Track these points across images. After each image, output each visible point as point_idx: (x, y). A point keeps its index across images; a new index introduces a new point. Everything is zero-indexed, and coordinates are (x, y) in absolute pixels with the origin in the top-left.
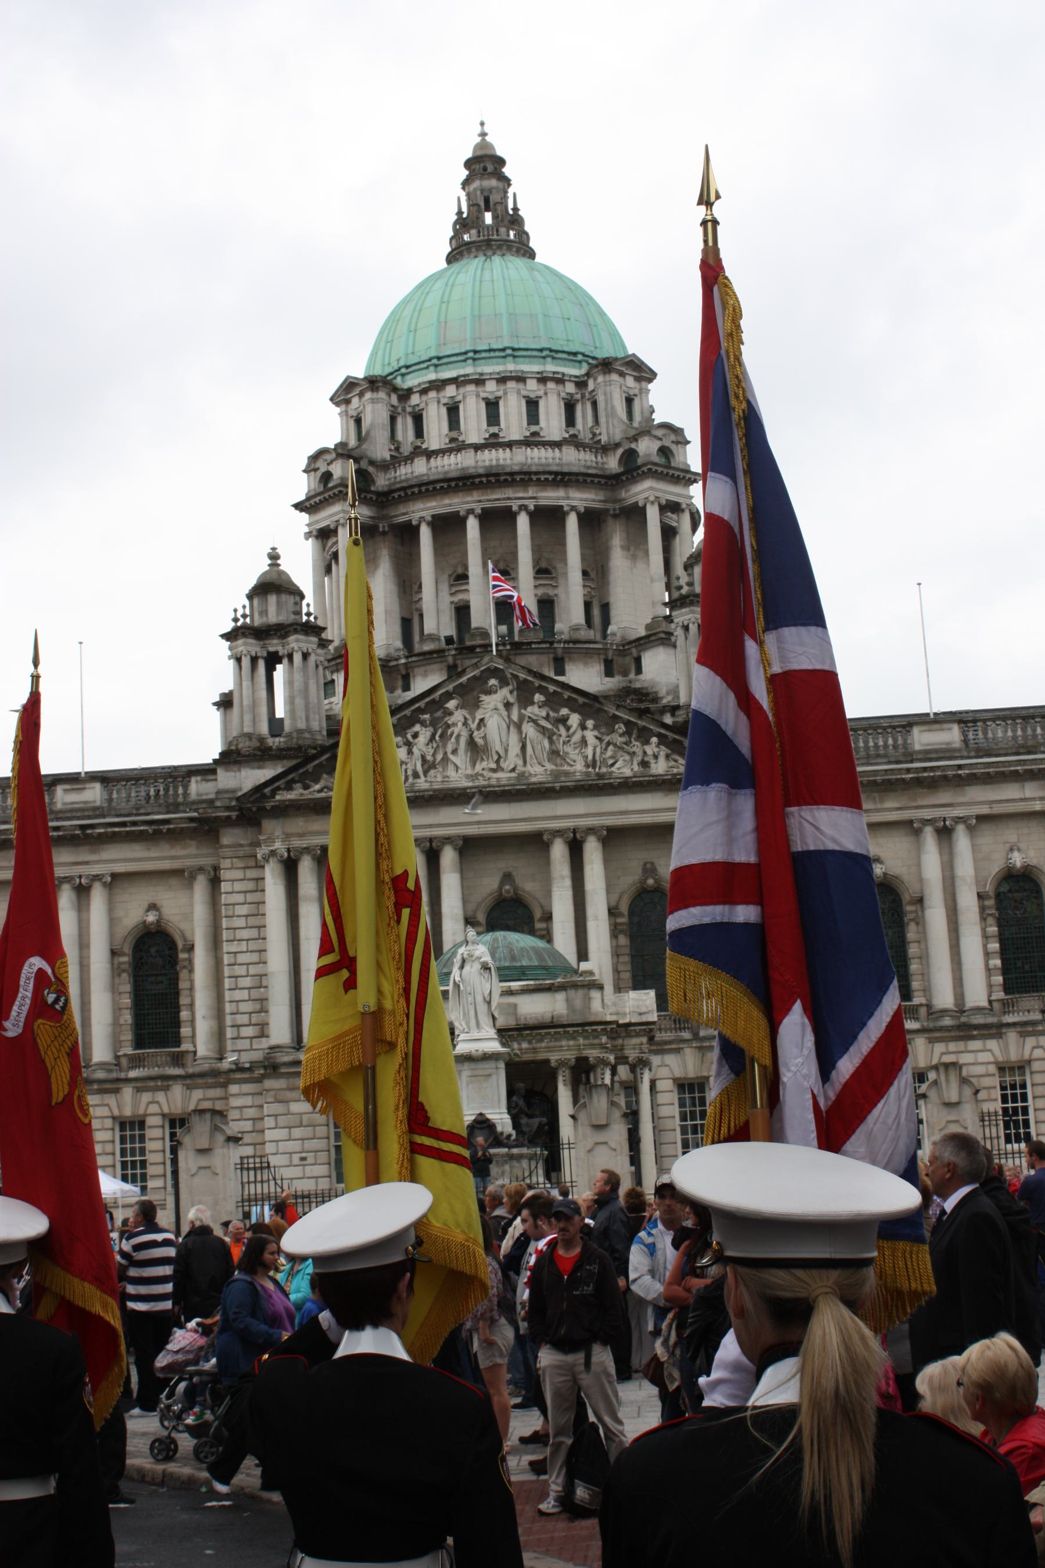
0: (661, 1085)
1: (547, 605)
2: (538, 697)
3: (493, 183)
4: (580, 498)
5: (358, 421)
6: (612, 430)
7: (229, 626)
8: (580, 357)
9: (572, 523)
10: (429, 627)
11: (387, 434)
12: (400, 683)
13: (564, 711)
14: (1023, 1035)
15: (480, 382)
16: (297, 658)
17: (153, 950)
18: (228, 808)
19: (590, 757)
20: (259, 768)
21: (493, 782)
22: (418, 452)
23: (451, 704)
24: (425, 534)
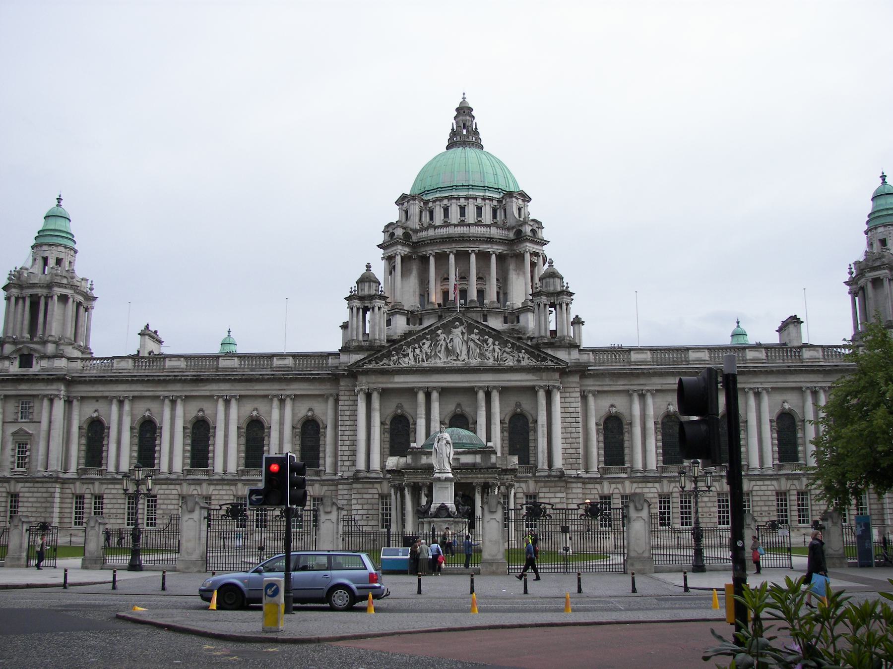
0: (518, 495)
1: (481, 293)
2: (476, 331)
3: (468, 118)
4: (497, 249)
5: (406, 212)
6: (511, 222)
7: (348, 294)
8: (500, 190)
9: (494, 257)
10: (433, 298)
11: (418, 218)
12: (418, 321)
13: (486, 337)
14: (670, 482)
16: (376, 309)
17: (310, 427)
18: (345, 370)
19: (496, 357)
21: (455, 365)
22: (430, 226)
23: (439, 332)
24: (432, 260)
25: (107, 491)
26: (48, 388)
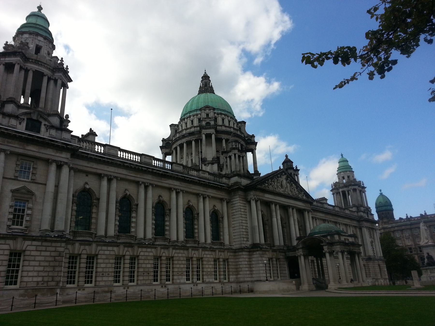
2: (289, 179)
15: (228, 117)
20: (244, 179)
25: (101, 252)
26: (58, 155)
